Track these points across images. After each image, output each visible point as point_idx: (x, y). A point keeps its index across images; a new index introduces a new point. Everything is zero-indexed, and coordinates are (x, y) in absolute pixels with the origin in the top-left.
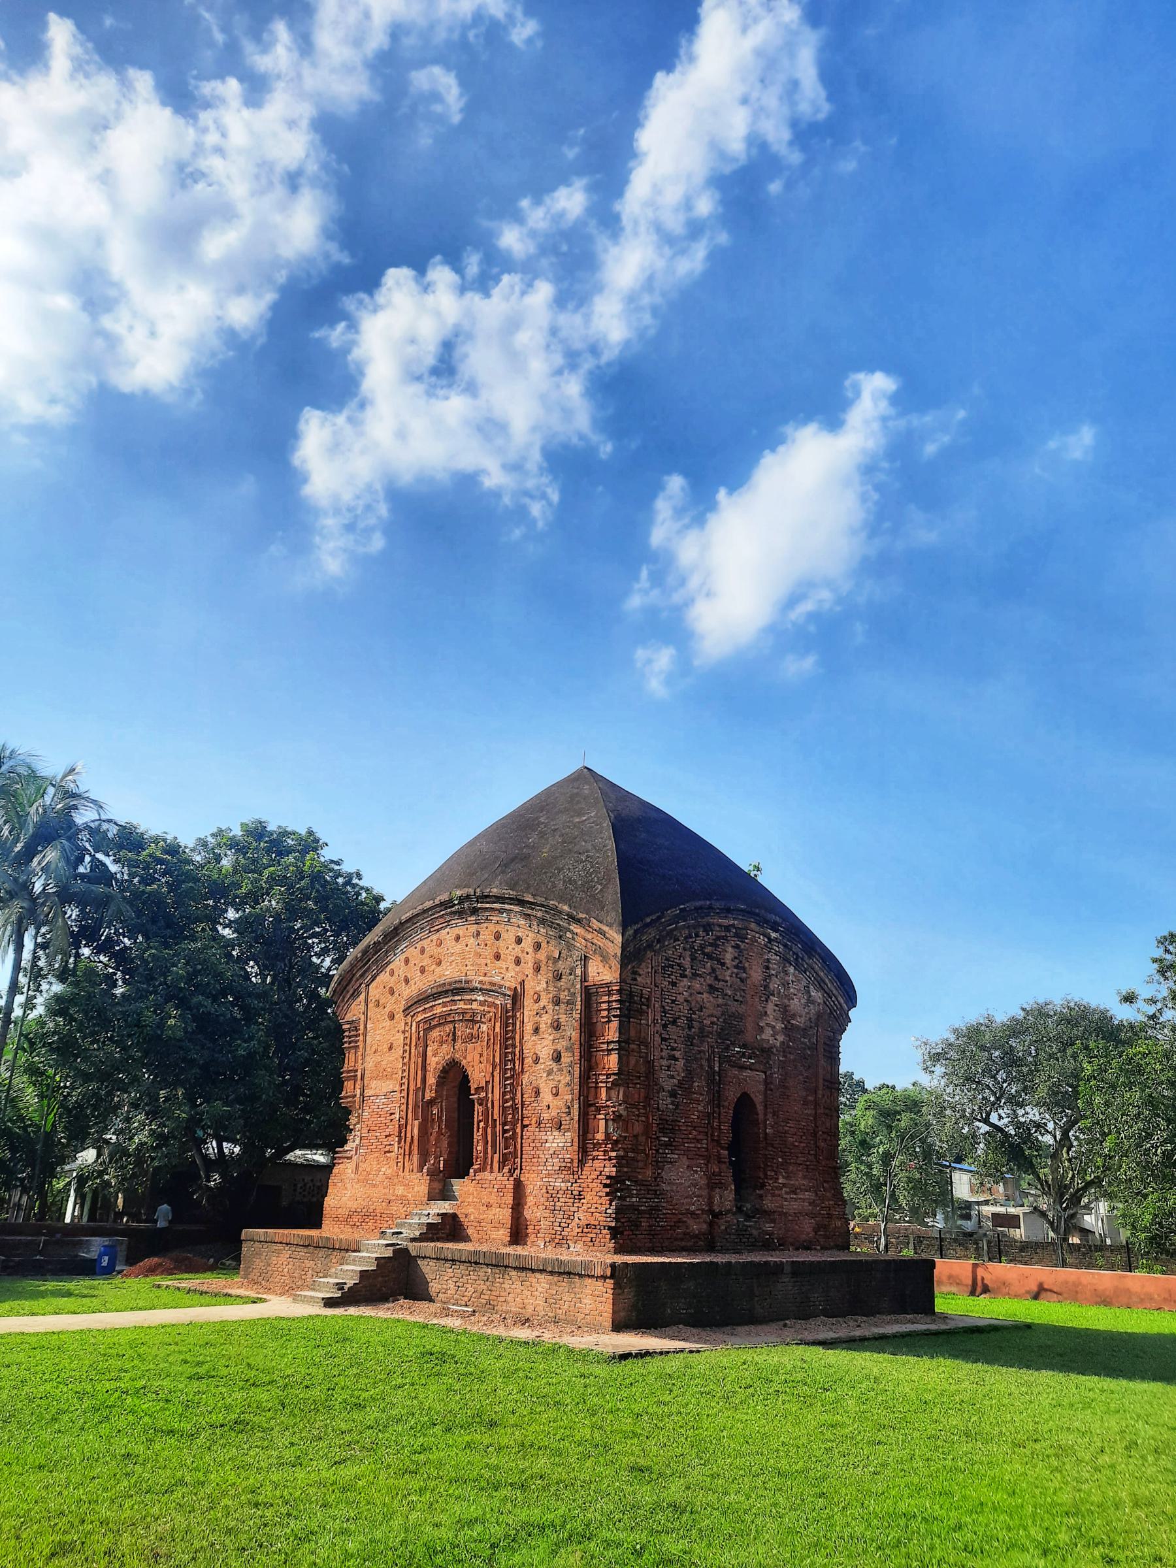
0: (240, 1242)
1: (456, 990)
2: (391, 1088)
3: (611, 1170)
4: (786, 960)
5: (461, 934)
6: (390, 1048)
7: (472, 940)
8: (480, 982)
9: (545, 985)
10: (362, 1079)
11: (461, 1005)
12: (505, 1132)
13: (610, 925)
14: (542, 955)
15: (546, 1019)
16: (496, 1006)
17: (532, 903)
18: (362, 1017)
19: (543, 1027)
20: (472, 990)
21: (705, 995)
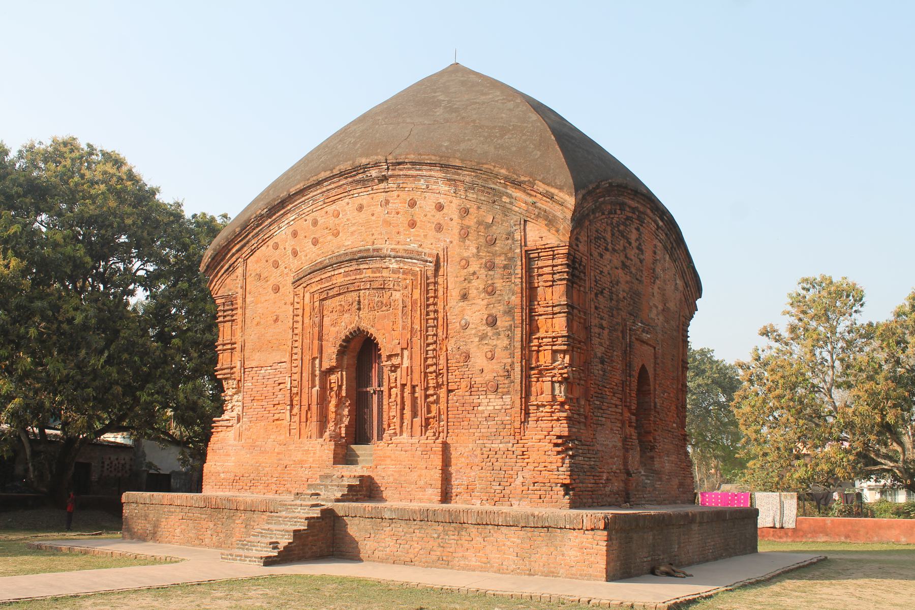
0: (120, 506)
1: (360, 258)
3: (562, 428)
4: (665, 248)
5: (365, 203)
6: (276, 320)
7: (379, 209)
8: (392, 250)
9: (475, 251)
12: (427, 396)
13: (561, 188)
14: (471, 221)
15: (478, 284)
16: (414, 274)
17: (460, 168)
18: (240, 291)
19: (473, 293)
20: (383, 257)
21: (620, 271)
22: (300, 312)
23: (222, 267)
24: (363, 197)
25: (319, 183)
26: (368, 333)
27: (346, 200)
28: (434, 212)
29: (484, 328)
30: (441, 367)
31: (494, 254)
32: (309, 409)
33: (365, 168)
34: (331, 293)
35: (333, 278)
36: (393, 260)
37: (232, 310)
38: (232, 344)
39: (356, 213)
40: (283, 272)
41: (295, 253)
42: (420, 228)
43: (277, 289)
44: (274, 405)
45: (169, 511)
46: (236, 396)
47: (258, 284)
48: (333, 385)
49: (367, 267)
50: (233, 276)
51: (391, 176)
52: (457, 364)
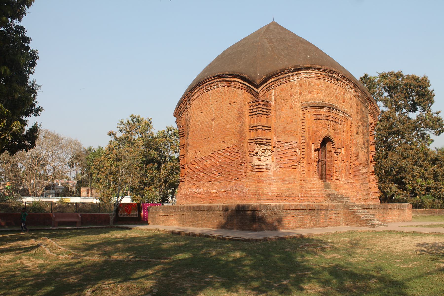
1: (331, 108)
7: (334, 90)
24: (329, 83)
25: (315, 69)
27: (322, 81)
33: (334, 72)
34: (319, 118)
37: (267, 109)
38: (267, 127)
41: (301, 94)
43: (291, 108)
45: (287, 213)
51: (340, 80)
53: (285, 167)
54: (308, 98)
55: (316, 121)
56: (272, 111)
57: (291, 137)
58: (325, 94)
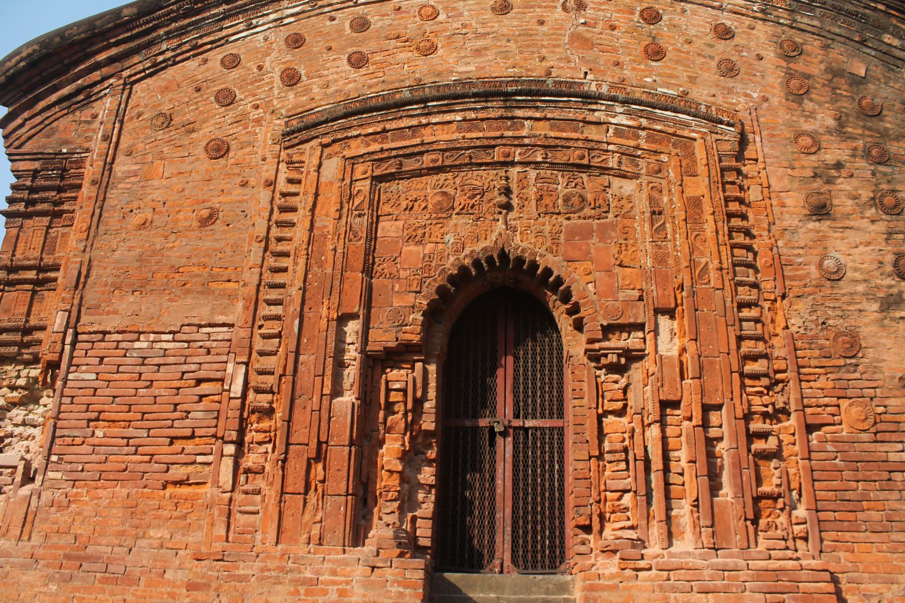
2: (203, 313)
7: (559, 13)
9: (831, 122)
10: (80, 283)
11: (542, 129)
18: (97, 146)
19: (843, 204)
22: (303, 203)
23: (55, 89)
26: (534, 265)
28: (710, 38)
29: (889, 281)
30: (781, 365)
31: (884, 134)
32: (320, 456)
34: (410, 165)
35: (427, 131)
36: (619, 109)
37: (60, 190)
38: (40, 269)
39: (489, 15)
40: (245, 115)
41: (291, 79)
42: (677, 62)
44: (173, 440)
46: (18, 414)
47: (160, 135)
48: (395, 397)
49: (538, 115)
50: (84, 115)
52: (825, 362)
53: (123, 475)
54: (334, 80)
55: (394, 186)
56: (87, 190)
57: (189, 300)
58: (481, 43)
